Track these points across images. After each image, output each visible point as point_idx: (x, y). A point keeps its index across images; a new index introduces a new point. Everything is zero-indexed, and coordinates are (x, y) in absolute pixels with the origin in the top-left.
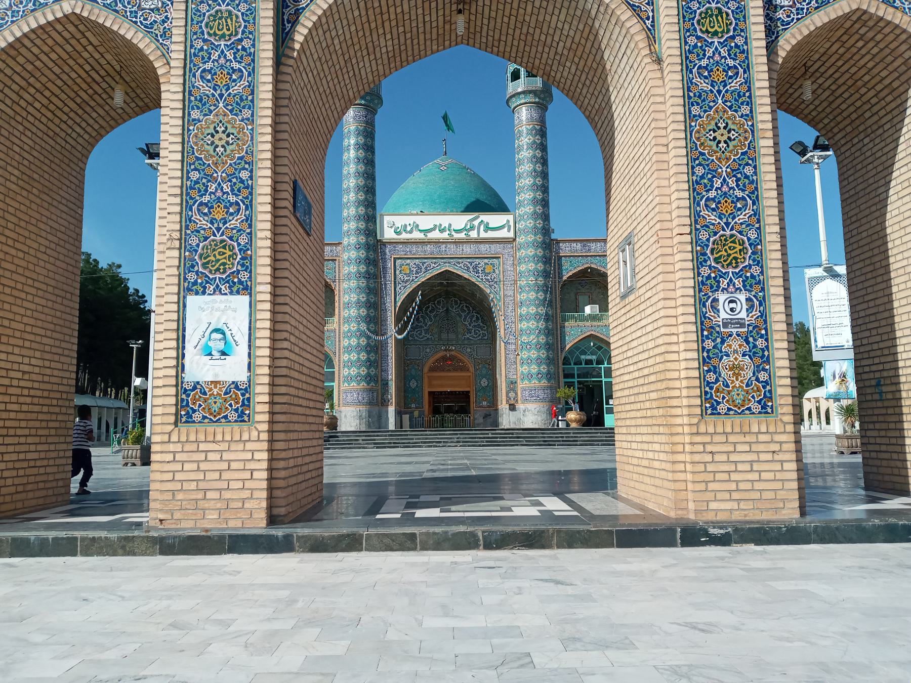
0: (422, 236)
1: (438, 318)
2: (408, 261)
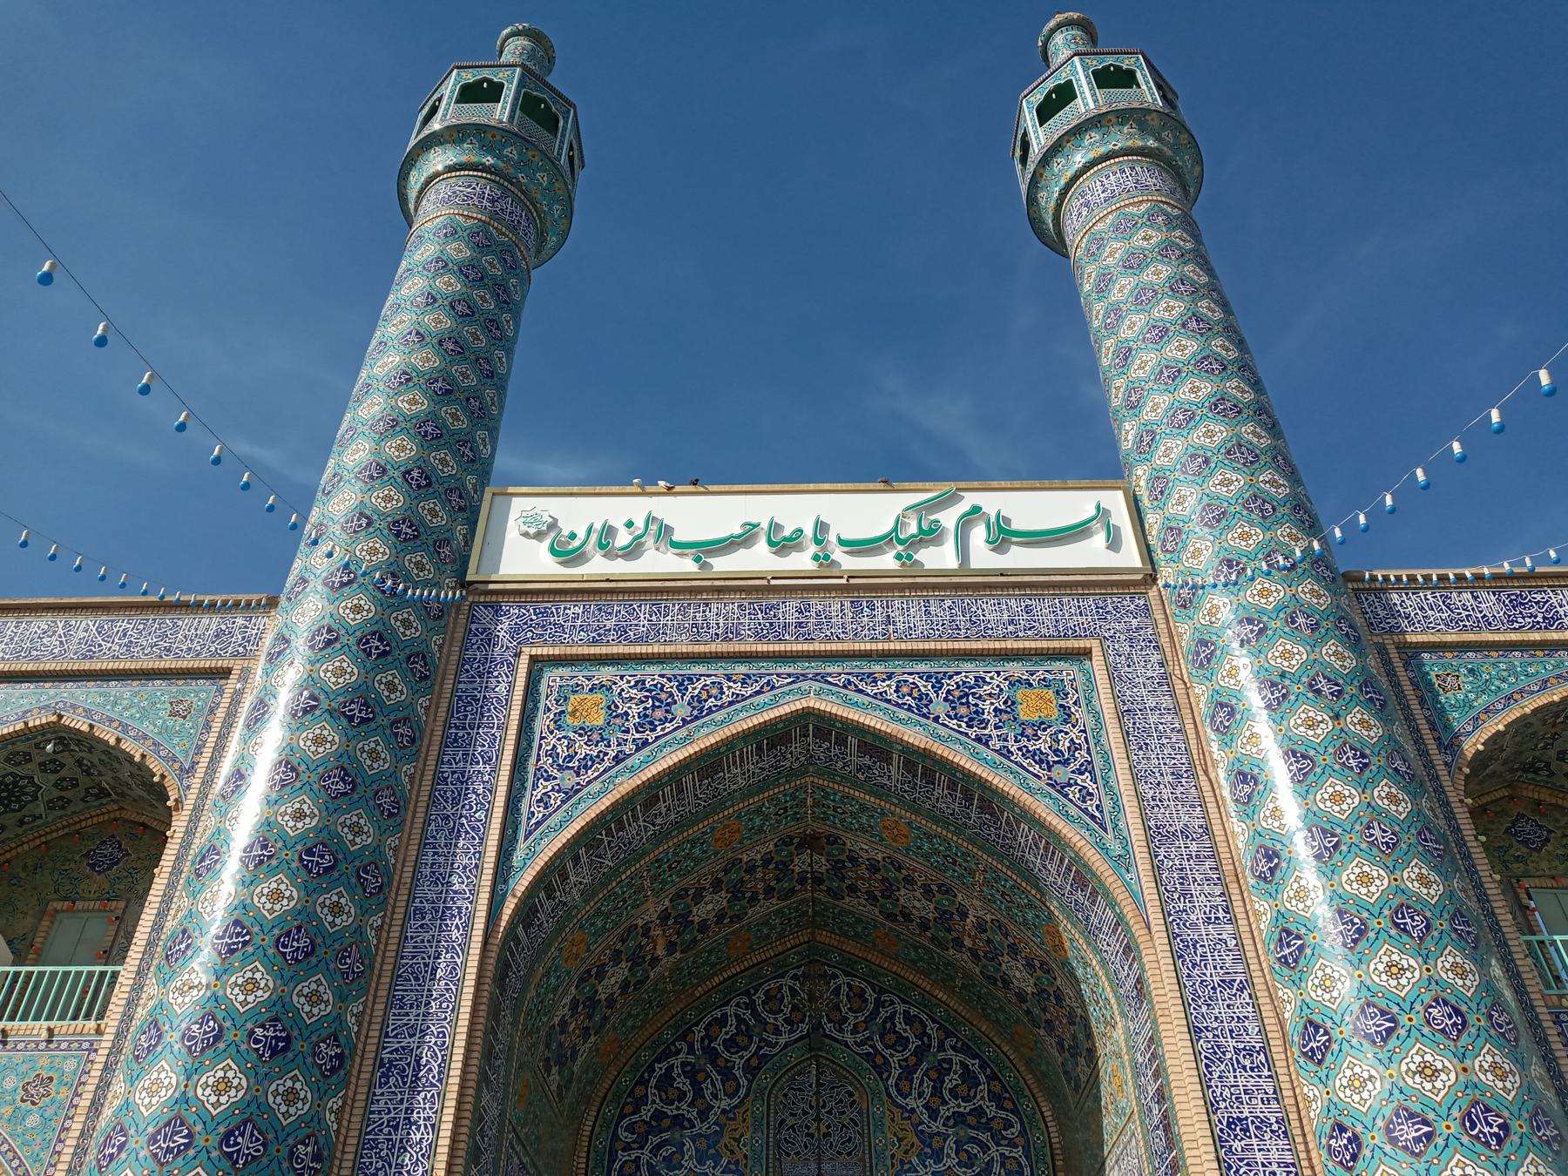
1: (764, 1079)
2: (606, 673)
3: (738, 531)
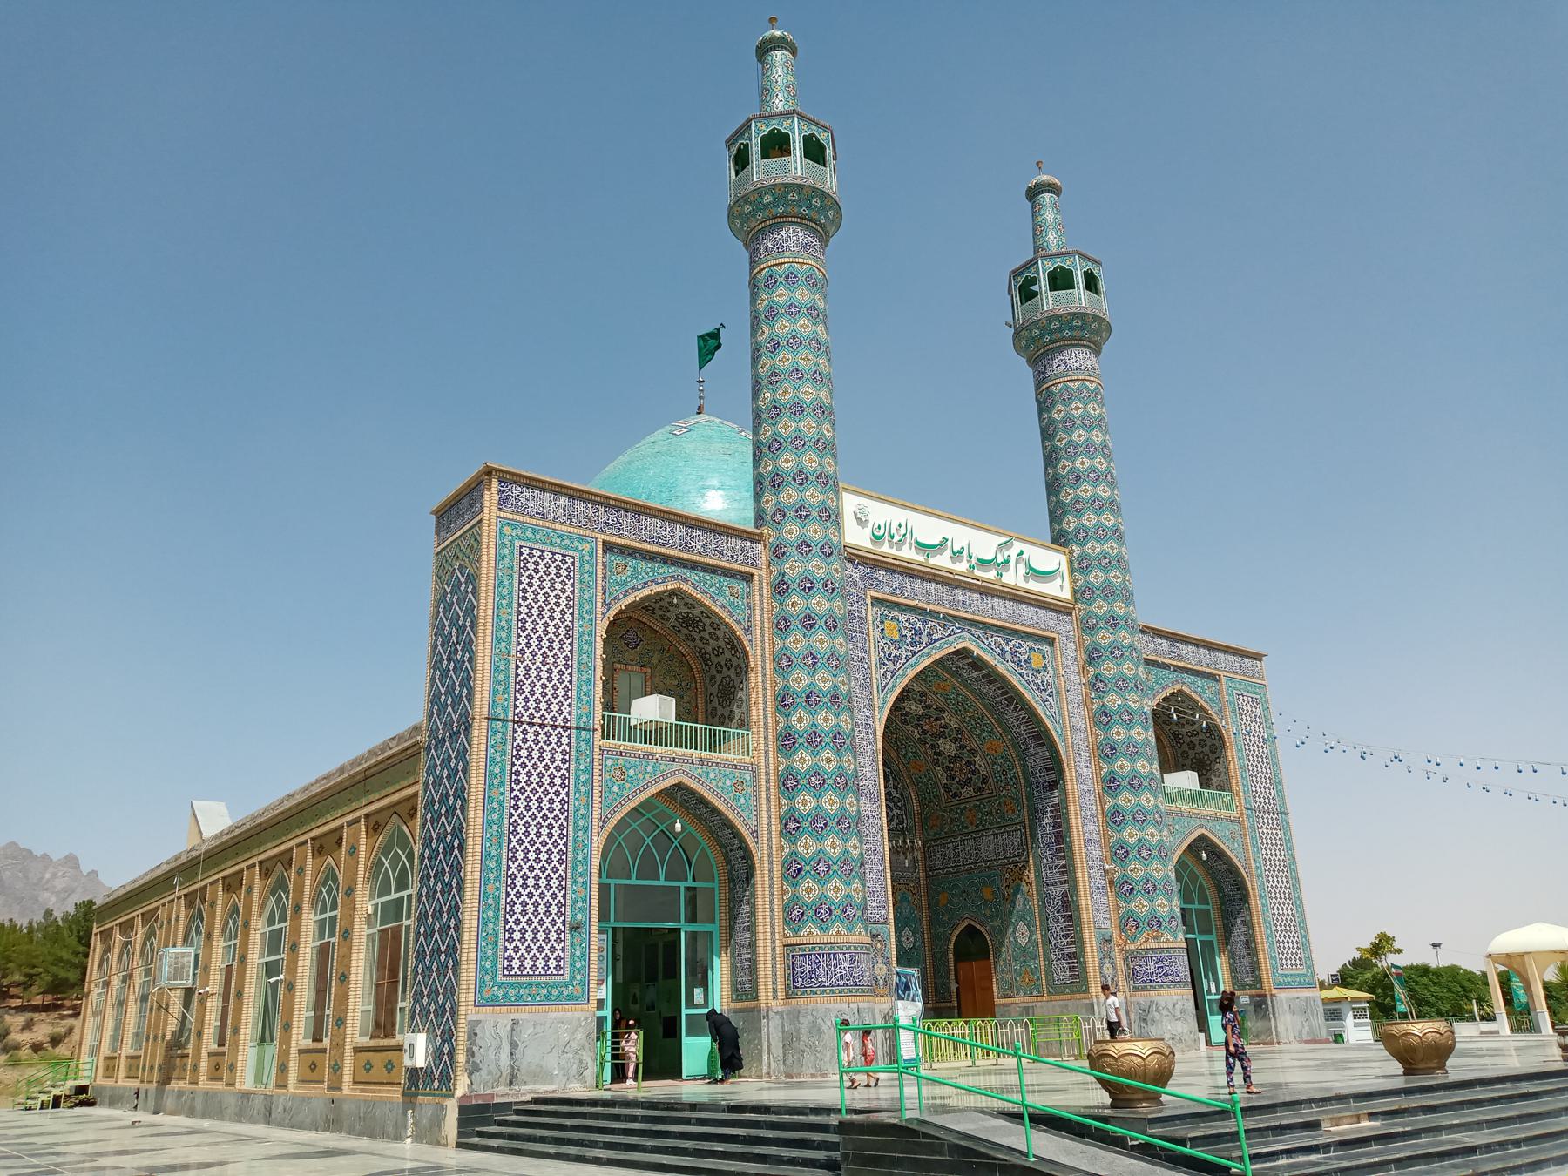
0: (920, 558)
3: (936, 542)
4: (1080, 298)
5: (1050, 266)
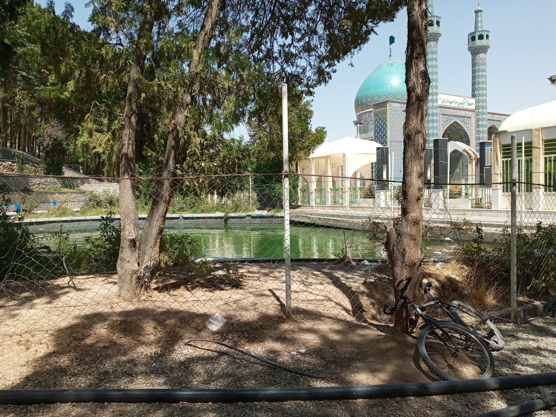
0: (449, 105)
4: (484, 42)
5: (479, 34)
